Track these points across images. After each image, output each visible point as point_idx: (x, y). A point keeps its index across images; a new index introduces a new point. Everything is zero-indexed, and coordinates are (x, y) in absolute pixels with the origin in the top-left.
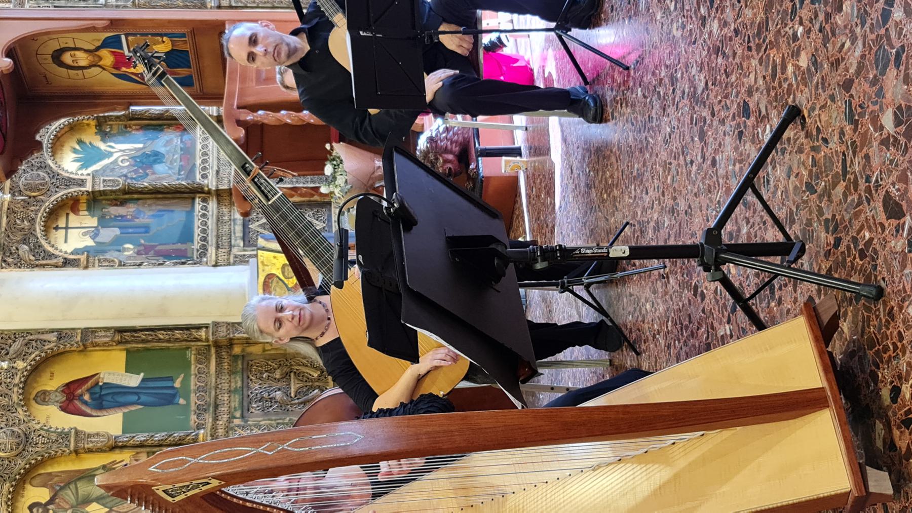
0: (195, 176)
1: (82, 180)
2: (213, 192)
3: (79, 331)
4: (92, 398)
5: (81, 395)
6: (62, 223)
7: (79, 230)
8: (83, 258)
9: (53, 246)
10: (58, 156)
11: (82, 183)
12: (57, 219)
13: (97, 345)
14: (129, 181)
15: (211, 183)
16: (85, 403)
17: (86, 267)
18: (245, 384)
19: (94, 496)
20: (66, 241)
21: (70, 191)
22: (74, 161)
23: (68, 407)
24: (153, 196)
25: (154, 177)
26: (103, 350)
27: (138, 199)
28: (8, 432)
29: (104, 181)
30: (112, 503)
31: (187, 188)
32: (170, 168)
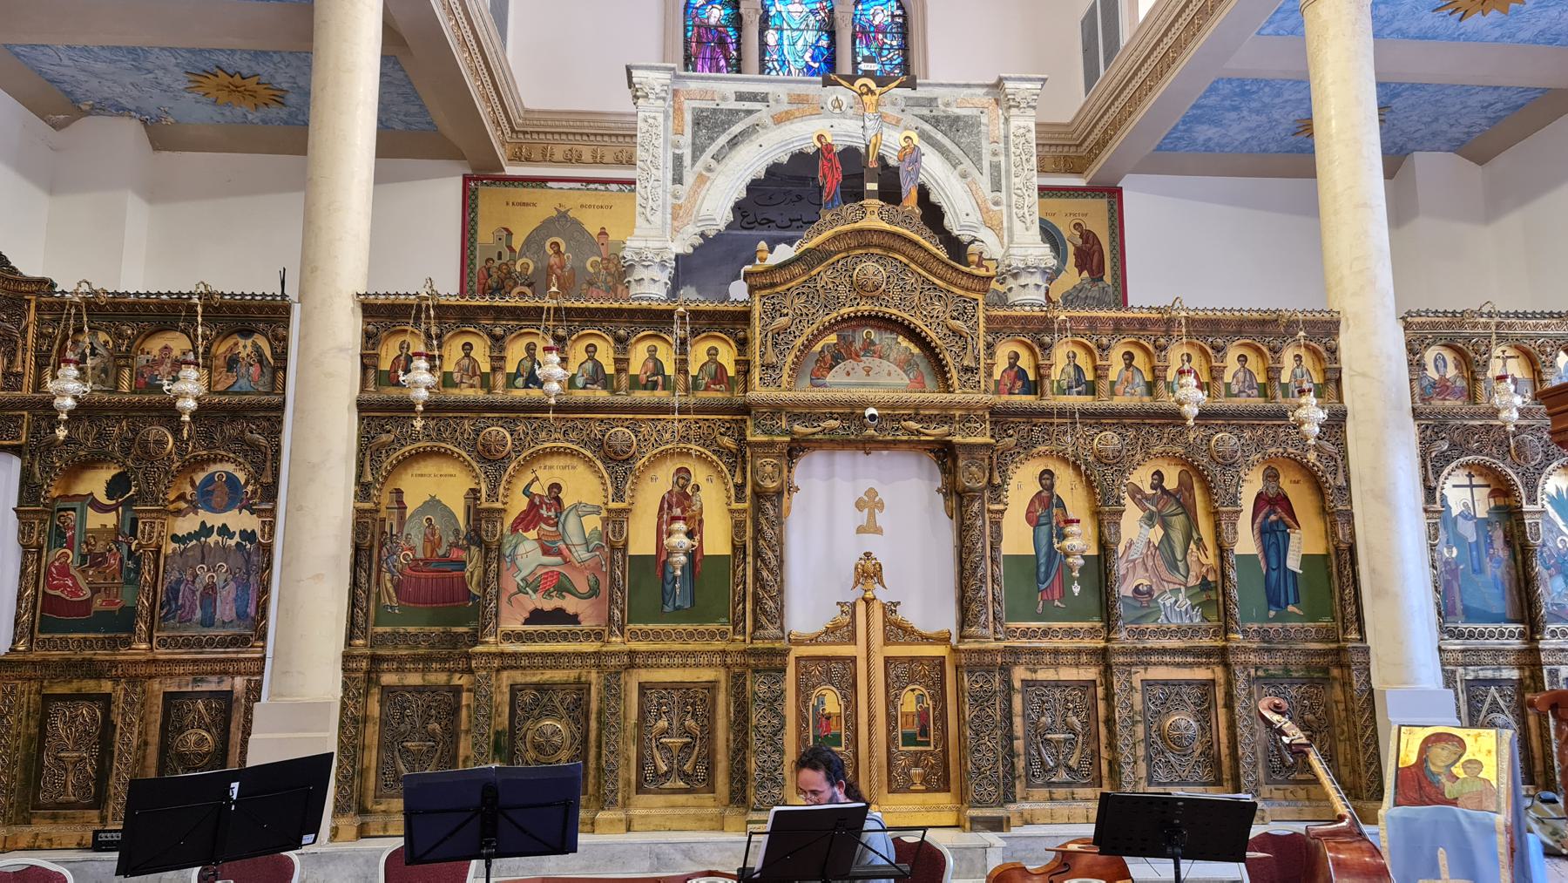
0: (1552, 622)
1: (1535, 500)
2: (1535, 644)
3: (1349, 508)
4: (1272, 522)
5: (1275, 512)
6: (1476, 481)
7: (1470, 499)
8: (1438, 507)
9: (1449, 474)
10: (1561, 471)
11: (1532, 499)
12: (1481, 475)
13: (1334, 524)
14: (1539, 549)
15: (1547, 643)
16: (1267, 516)
17: (1426, 510)
18: (1296, 681)
19: (1170, 531)
20: (1454, 486)
21: (1521, 487)
22: (1557, 488)
23: (1260, 500)
24: (1522, 577)
25: (1547, 576)
26: (1326, 531)
27: (1515, 560)
28: (1236, 447)
29: (1537, 524)
30: (1163, 549)
31: (1537, 614)
32: (1559, 593)
